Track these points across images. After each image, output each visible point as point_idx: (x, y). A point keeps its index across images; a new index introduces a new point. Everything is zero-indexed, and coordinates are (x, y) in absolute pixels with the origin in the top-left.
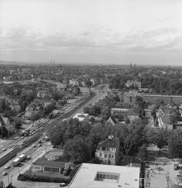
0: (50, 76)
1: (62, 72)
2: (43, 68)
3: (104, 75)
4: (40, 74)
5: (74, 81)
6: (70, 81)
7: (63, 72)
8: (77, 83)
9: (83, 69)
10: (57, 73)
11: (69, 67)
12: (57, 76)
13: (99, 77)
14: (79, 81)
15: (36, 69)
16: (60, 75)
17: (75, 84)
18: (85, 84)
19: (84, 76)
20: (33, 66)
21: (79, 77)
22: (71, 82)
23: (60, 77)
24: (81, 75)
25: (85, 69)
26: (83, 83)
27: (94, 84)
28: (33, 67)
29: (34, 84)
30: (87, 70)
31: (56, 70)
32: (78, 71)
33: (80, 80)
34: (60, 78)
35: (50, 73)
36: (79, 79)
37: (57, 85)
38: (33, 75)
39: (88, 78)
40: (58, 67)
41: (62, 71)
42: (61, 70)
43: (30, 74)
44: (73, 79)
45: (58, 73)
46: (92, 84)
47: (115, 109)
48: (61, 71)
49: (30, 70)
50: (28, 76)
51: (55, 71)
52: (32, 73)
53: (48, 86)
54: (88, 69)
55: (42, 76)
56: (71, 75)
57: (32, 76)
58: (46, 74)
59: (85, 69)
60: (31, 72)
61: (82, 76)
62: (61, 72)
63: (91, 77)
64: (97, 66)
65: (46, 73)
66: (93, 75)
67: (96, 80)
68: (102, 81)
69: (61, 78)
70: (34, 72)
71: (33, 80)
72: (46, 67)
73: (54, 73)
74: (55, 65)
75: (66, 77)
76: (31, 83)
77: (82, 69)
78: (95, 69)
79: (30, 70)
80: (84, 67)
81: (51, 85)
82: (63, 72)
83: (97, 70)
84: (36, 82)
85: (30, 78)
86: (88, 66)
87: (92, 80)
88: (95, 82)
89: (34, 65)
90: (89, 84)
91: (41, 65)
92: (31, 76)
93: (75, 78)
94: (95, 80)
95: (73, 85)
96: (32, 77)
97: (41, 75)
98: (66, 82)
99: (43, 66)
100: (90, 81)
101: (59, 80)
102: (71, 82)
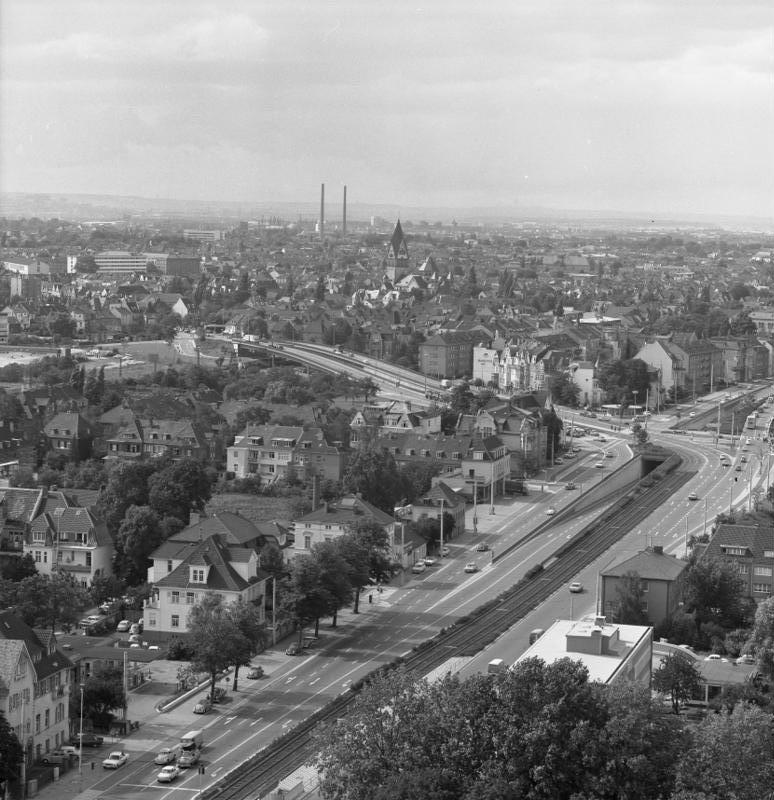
0: (318, 315)
1: (409, 283)
2: (258, 245)
3: (751, 315)
4: (243, 297)
5: (513, 354)
6: (479, 352)
7: (418, 280)
8: (533, 374)
9: (576, 261)
10: (374, 294)
11: (460, 243)
12: (371, 311)
13: (712, 332)
14: (547, 357)
15: (209, 259)
16: (392, 304)
17: (514, 378)
18: (602, 381)
19: (590, 319)
20: (186, 233)
21: (546, 325)
22: (485, 365)
23: (397, 322)
24: (560, 313)
25: (591, 261)
26: (584, 378)
27: (668, 380)
28: (182, 240)
29: (202, 376)
30: (601, 272)
31: (364, 264)
32: (533, 276)
33: (560, 351)
34: (394, 327)
35: (320, 292)
36: (553, 342)
37: (375, 388)
38: (186, 302)
39: (617, 339)
40: (373, 241)
41: (410, 278)
42: (401, 264)
43: (167, 298)
44: (499, 341)
45: (382, 294)
46: (654, 385)
47: (41, 494)
48: (403, 276)
49: (163, 266)
50: (151, 309)
51: (356, 273)
52: (177, 288)
53: (310, 391)
54: (617, 266)
55: (262, 314)
56: (486, 312)
57: (180, 308)
58: (286, 299)
59: (591, 261)
60: (167, 279)
61: (571, 317)
62: (403, 283)
63: (637, 325)
64: (679, 242)
65: (290, 291)
66: (655, 316)
67: (688, 349)
68: (732, 360)
69: (408, 331)
70: (191, 281)
71: (186, 344)
72: (280, 244)
73: (347, 291)
74: (356, 224)
75: (444, 324)
76: (178, 368)
77: (563, 265)
78: (669, 261)
79: (163, 266)
80: (575, 246)
81: (332, 385)
82: (415, 285)
83: (686, 273)
84: (209, 360)
85: (168, 329)
86: (612, 241)
87: (654, 355)
88: (677, 369)
89: (194, 225)
90: (629, 385)
91: (244, 225)
92: (168, 308)
93: (515, 333)
94: (676, 350)
95: (503, 385)
96: (177, 320)
97: (250, 303)
98: (448, 362)
99: (256, 233)
100: (637, 357)
101: (389, 344)
102: (485, 365)
